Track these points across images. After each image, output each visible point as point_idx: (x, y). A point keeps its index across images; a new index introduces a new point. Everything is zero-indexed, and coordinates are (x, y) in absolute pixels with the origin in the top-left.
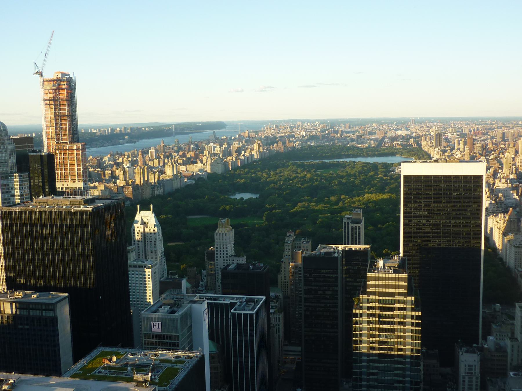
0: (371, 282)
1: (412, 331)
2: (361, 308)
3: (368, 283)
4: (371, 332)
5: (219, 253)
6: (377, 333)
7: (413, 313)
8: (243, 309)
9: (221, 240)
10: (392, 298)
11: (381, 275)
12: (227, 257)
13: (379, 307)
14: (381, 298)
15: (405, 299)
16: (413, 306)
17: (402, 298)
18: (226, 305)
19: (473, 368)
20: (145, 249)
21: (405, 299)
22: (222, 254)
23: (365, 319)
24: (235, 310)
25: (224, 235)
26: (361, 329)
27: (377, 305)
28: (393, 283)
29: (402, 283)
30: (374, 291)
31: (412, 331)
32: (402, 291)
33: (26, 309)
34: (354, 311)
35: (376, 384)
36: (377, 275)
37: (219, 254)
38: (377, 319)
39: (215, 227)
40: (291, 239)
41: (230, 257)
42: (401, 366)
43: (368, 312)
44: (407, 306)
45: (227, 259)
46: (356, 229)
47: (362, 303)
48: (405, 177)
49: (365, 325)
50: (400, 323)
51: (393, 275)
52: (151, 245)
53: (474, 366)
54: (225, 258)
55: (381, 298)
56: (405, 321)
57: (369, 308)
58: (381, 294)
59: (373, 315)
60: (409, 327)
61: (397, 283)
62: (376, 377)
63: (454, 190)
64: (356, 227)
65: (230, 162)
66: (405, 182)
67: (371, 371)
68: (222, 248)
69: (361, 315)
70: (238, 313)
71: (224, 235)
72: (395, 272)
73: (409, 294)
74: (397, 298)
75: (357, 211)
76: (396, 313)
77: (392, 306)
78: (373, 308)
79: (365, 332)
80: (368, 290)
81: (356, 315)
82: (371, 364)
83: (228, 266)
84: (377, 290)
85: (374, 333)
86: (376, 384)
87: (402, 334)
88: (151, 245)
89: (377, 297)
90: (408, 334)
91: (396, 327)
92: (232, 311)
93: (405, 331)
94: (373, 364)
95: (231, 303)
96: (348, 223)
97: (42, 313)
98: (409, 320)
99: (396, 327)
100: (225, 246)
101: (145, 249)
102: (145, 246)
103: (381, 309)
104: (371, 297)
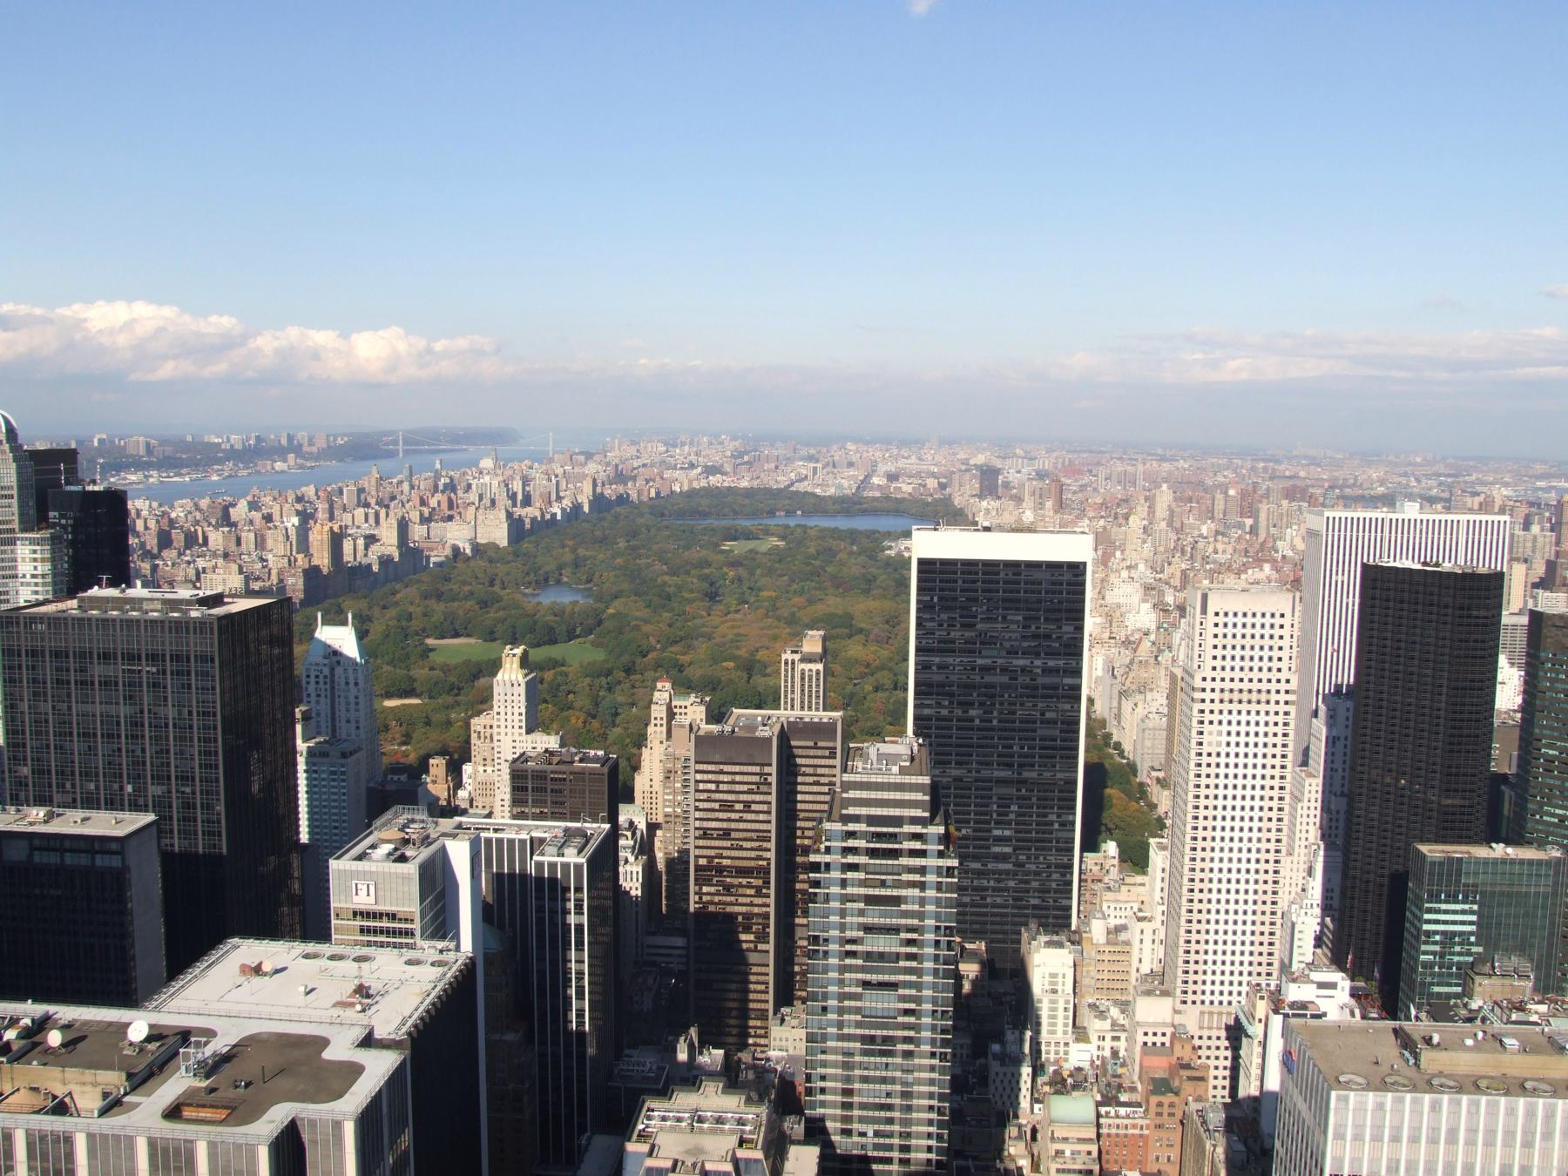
0: (852, 794)
1: (938, 902)
2: (828, 850)
3: (845, 795)
5: (503, 723)
7: (941, 862)
9: (509, 694)
10: (897, 830)
11: (873, 779)
12: (520, 734)
13: (867, 849)
14: (873, 829)
15: (924, 831)
16: (942, 848)
17: (918, 829)
18: (523, 842)
19: (1060, 979)
20: (333, 714)
22: (510, 727)
23: (836, 874)
24: (542, 854)
27: (861, 843)
28: (898, 796)
29: (919, 796)
30: (857, 812)
31: (938, 902)
32: (919, 813)
33: (54, 850)
35: (859, 1018)
36: (865, 779)
37: (503, 726)
38: (862, 875)
39: (495, 666)
40: (666, 696)
41: (527, 733)
42: (914, 978)
43: (844, 861)
46: (810, 678)
48: (921, 562)
49: (835, 890)
50: (913, 884)
51: (899, 779)
52: (348, 704)
53: (1060, 976)
54: (518, 738)
55: (873, 829)
57: (847, 851)
58: (872, 821)
59: (854, 867)
60: (931, 893)
61: (908, 796)
62: (859, 1004)
64: (810, 670)
65: (527, 521)
66: (920, 572)
67: (847, 989)
69: (828, 865)
72: (903, 771)
73: (930, 821)
74: (908, 829)
75: (812, 636)
76: (904, 861)
77: (896, 846)
78: (853, 851)
79: (835, 904)
80: (844, 812)
82: (847, 975)
84: (863, 811)
86: (859, 1018)
87: (916, 907)
88: (348, 704)
90: (930, 908)
91: (903, 892)
92: (535, 858)
93: (922, 901)
94: (853, 976)
95: (532, 839)
97: (93, 860)
98: (931, 878)
99: (903, 892)
101: (333, 714)
102: (333, 708)
103: (872, 853)
104: (851, 827)
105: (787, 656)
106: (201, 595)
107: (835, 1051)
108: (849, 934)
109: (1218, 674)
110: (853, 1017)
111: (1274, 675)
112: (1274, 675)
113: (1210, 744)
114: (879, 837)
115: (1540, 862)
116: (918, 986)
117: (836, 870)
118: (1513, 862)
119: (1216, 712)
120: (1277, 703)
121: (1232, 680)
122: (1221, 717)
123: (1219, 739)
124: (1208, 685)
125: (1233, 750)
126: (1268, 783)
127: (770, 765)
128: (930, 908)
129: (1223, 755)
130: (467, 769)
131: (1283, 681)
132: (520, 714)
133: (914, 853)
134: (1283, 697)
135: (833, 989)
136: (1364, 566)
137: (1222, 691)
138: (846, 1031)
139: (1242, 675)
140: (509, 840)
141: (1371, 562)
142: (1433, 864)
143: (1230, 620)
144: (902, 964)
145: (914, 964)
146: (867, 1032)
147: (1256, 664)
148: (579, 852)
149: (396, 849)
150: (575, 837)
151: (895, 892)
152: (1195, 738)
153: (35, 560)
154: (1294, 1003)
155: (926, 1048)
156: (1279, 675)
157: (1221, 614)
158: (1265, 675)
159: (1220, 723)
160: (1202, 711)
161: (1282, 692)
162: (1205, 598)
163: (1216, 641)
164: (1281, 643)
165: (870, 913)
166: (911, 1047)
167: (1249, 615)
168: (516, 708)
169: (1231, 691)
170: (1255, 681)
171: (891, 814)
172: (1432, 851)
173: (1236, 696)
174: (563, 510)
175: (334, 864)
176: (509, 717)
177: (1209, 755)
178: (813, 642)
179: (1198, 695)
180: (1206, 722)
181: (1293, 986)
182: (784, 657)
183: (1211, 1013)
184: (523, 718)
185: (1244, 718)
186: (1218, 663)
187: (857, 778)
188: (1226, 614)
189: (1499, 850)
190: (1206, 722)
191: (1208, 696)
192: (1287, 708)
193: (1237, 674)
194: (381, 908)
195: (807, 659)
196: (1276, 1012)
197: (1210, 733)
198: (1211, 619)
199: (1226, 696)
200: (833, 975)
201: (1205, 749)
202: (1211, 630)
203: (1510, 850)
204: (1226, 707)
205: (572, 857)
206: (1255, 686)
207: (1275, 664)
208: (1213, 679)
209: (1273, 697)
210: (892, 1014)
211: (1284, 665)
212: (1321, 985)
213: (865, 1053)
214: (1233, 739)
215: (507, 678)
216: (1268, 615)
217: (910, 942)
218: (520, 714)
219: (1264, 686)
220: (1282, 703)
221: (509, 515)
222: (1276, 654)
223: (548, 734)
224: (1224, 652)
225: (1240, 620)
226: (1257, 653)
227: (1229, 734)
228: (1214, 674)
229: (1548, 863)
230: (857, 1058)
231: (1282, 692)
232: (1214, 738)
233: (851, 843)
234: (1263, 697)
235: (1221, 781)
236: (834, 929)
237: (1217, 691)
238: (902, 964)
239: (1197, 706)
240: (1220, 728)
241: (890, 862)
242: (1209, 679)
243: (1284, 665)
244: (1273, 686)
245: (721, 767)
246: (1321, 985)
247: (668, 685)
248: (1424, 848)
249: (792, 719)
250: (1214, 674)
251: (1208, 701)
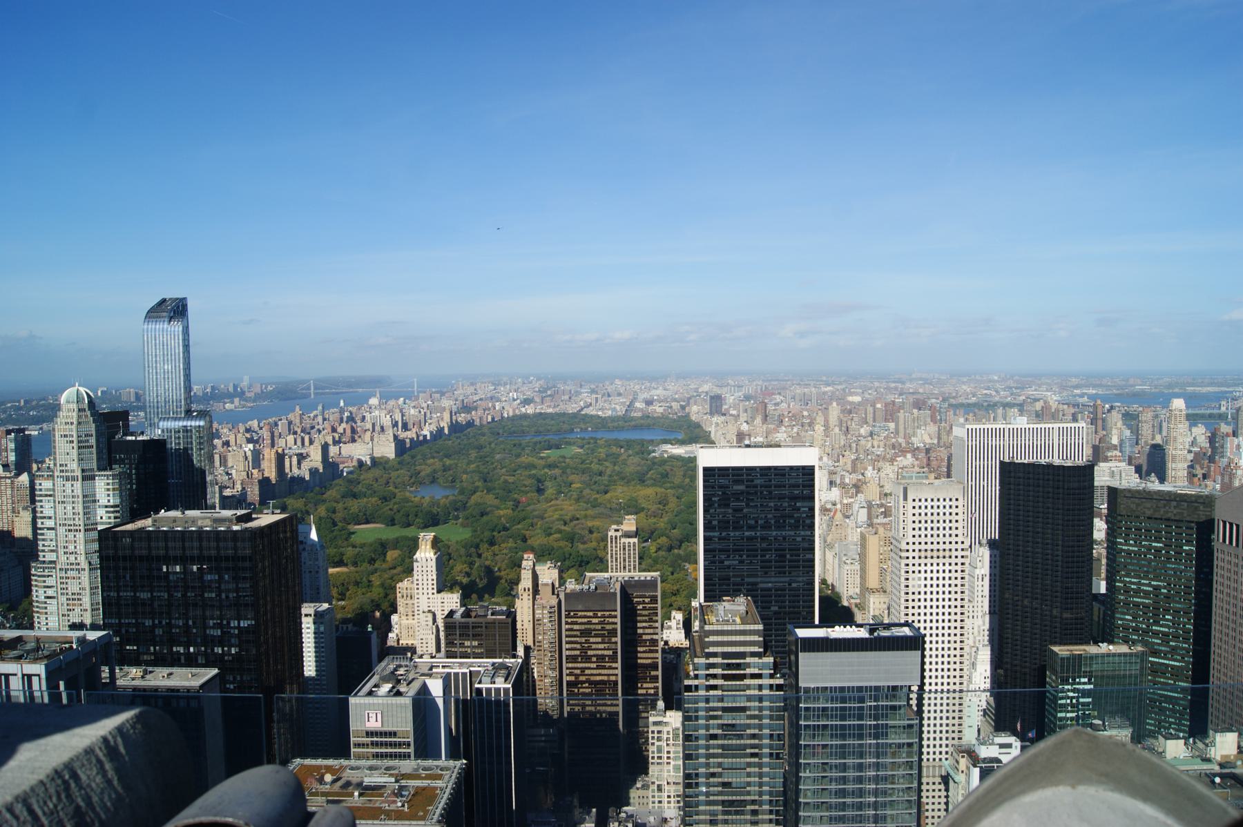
0: (712, 638)
2: (696, 677)
3: (707, 639)
4: (711, 713)
5: (420, 587)
6: (720, 713)
7: (772, 681)
10: (742, 661)
11: (725, 628)
12: (433, 594)
14: (726, 661)
17: (756, 660)
18: (464, 674)
21: (760, 661)
23: (702, 693)
24: (480, 682)
25: (429, 560)
26: (697, 710)
27: (719, 671)
28: (742, 638)
29: (756, 638)
30: (715, 651)
31: (771, 709)
32: (756, 649)
34: (687, 682)
36: (719, 628)
37: (421, 589)
38: (719, 693)
39: (414, 546)
40: (531, 563)
43: (707, 683)
44: (764, 672)
45: (433, 596)
46: (629, 546)
47: (697, 670)
48: (705, 469)
51: (742, 627)
55: (726, 661)
56: (760, 693)
57: (708, 676)
58: (725, 655)
59: (714, 687)
60: (766, 704)
61: (748, 638)
63: (775, 487)
64: (629, 543)
65: (408, 441)
67: (712, 770)
68: (425, 580)
69: (697, 688)
70: (487, 689)
71: (429, 560)
74: (748, 660)
75: (629, 520)
76: (747, 682)
77: (742, 672)
78: (714, 676)
80: (707, 650)
81: (688, 688)
82: (711, 760)
83: (452, 613)
85: (715, 713)
87: (757, 713)
89: (719, 660)
90: (766, 712)
91: (748, 704)
93: (761, 709)
94: (716, 760)
95: (470, 671)
96: (616, 538)
98: (766, 692)
100: (430, 577)
103: (725, 677)
104: (712, 660)
105: (611, 533)
106: (239, 514)
107: (704, 813)
108: (712, 732)
109: (917, 540)
110: (716, 789)
111: (953, 539)
112: (953, 539)
113: (913, 586)
114: (729, 666)
115: (1131, 655)
116: (760, 765)
117: (702, 690)
118: (1114, 655)
119: (917, 565)
120: (956, 557)
121: (926, 543)
122: (920, 568)
123: (919, 582)
124: (911, 547)
125: (929, 589)
126: (953, 610)
127: (616, 611)
129: (922, 593)
130: (394, 618)
131: (960, 543)
132: (433, 580)
133: (754, 676)
134: (960, 553)
135: (702, 770)
136: (1001, 463)
137: (920, 550)
138: (712, 798)
139: (932, 540)
140: (454, 673)
141: (1007, 460)
142: (1062, 659)
143: (923, 504)
144: (748, 751)
145: (756, 751)
146: (726, 798)
147: (941, 532)
148: (506, 681)
149: (393, 687)
150: (501, 669)
151: (742, 705)
152: (904, 583)
153: (108, 490)
154: (985, 759)
155: (766, 807)
156: (957, 539)
157: (917, 500)
158: (947, 539)
159: (920, 572)
160: (907, 565)
161: (959, 550)
162: (905, 490)
163: (914, 518)
164: (957, 518)
165: (726, 717)
166: (756, 807)
167: (935, 500)
168: (430, 576)
169: (926, 550)
170: (941, 543)
171: (738, 651)
172: (1061, 650)
173: (929, 554)
174: (431, 433)
175: (353, 701)
176: (425, 582)
177: (913, 593)
178: (630, 524)
179: (904, 554)
180: (911, 572)
181: (983, 747)
182: (610, 534)
183: (934, 767)
184: (435, 582)
185: (935, 568)
186: (917, 533)
187: (715, 628)
189: (1104, 648)
190: (911, 572)
191: (910, 554)
192: (963, 560)
193: (929, 539)
194: (386, 729)
195: (627, 535)
196: (975, 766)
197: (913, 579)
198: (910, 503)
199: (923, 554)
200: (702, 760)
201: (910, 590)
202: (912, 511)
203: (1111, 647)
204: (923, 561)
205: (500, 684)
206: (941, 546)
207: (954, 532)
208: (914, 543)
209: (954, 553)
210: (742, 786)
211: (959, 532)
212: (1002, 746)
213: (725, 813)
214: (929, 582)
215: (423, 555)
216: (948, 500)
217: (754, 736)
218: (433, 580)
219: (947, 546)
220: (959, 557)
221: (395, 437)
222: (954, 525)
223: (452, 593)
224: (920, 525)
225: (929, 504)
226: (941, 525)
227: (926, 579)
229: (1136, 655)
230: (720, 817)
231: (959, 550)
232: (916, 583)
233: (712, 671)
234: (947, 553)
235: (922, 611)
236: (702, 729)
237: (917, 551)
238: (748, 751)
239: (904, 561)
240: (919, 575)
241: (738, 683)
242: (911, 543)
243: (959, 532)
244: (953, 546)
245: (586, 613)
246: (1002, 746)
247: (532, 556)
248: (1056, 649)
249: (626, 579)
251: (911, 558)
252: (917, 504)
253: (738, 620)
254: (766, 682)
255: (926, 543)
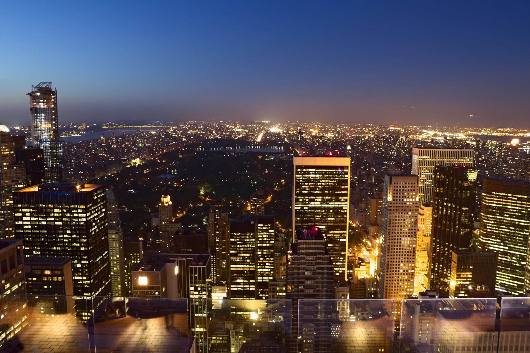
0: (301, 246)
3: (299, 247)
7: (328, 266)
8: (198, 265)
17: (321, 256)
29: (322, 246)
31: (327, 278)
32: (322, 251)
48: (296, 166)
60: (325, 276)
87: (321, 280)
98: (325, 271)
99: (317, 276)
121: (400, 203)
128: (325, 280)
153: (16, 173)
163: (394, 192)
188: (398, 183)
191: (392, 208)
198: (393, 185)
216: (410, 184)
228: (394, 202)
250: (394, 202)
252: (396, 185)
253: (314, 238)
254: (325, 266)
255: (400, 203)
